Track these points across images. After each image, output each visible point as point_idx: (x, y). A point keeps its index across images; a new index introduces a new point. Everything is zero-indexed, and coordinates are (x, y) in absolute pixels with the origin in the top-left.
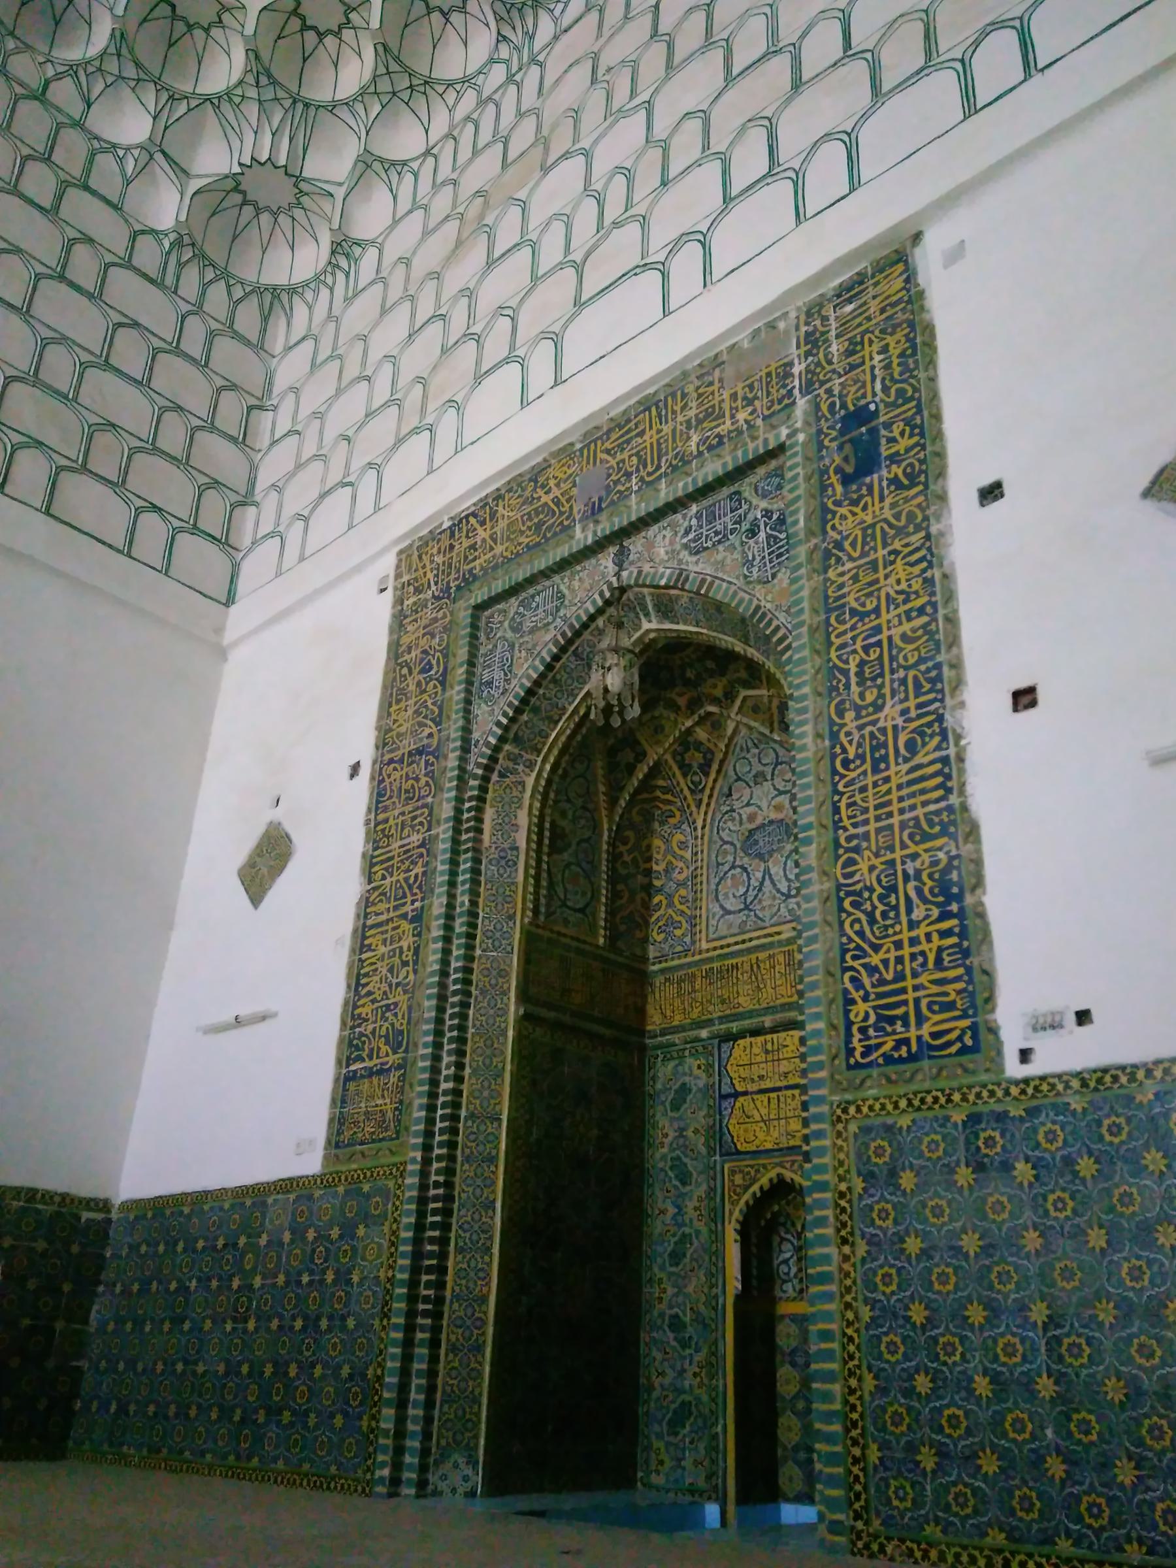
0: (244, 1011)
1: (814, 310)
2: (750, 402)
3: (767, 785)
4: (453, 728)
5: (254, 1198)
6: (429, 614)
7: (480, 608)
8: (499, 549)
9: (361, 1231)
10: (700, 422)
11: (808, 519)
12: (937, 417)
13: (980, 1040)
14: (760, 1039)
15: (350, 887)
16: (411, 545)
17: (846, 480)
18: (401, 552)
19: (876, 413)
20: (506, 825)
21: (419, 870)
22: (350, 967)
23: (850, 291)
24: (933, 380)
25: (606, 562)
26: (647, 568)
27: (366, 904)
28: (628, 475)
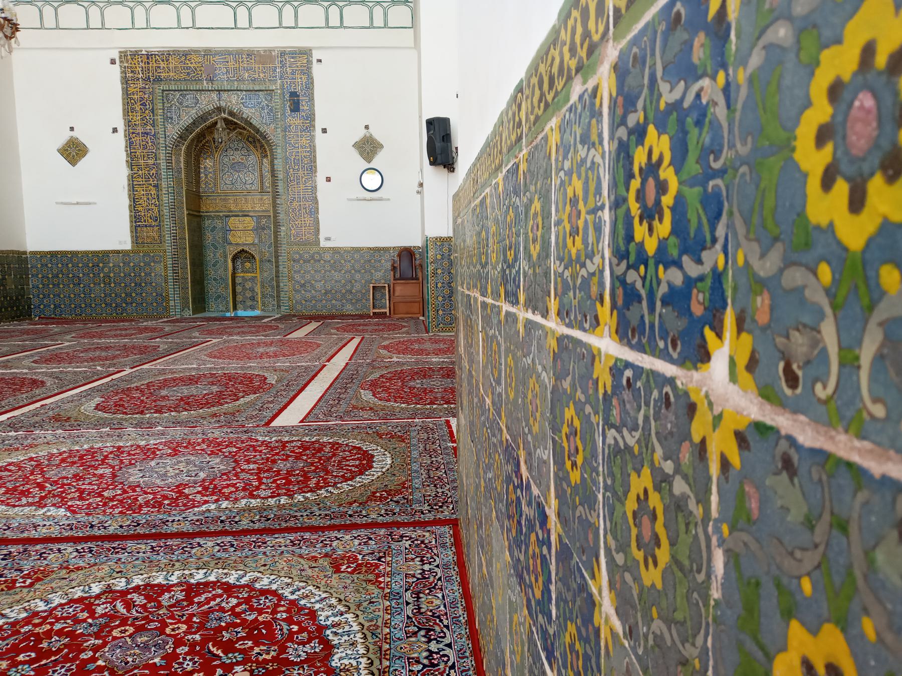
1: (283, 53)
2: (264, 73)
4: (161, 130)
5: (104, 255)
6: (141, 84)
7: (163, 91)
8: (172, 74)
9: (152, 264)
16: (126, 52)
17: (292, 111)
18: (120, 52)
19: (298, 96)
20: (178, 162)
21: (154, 171)
22: (130, 195)
25: (214, 96)
27: (132, 178)
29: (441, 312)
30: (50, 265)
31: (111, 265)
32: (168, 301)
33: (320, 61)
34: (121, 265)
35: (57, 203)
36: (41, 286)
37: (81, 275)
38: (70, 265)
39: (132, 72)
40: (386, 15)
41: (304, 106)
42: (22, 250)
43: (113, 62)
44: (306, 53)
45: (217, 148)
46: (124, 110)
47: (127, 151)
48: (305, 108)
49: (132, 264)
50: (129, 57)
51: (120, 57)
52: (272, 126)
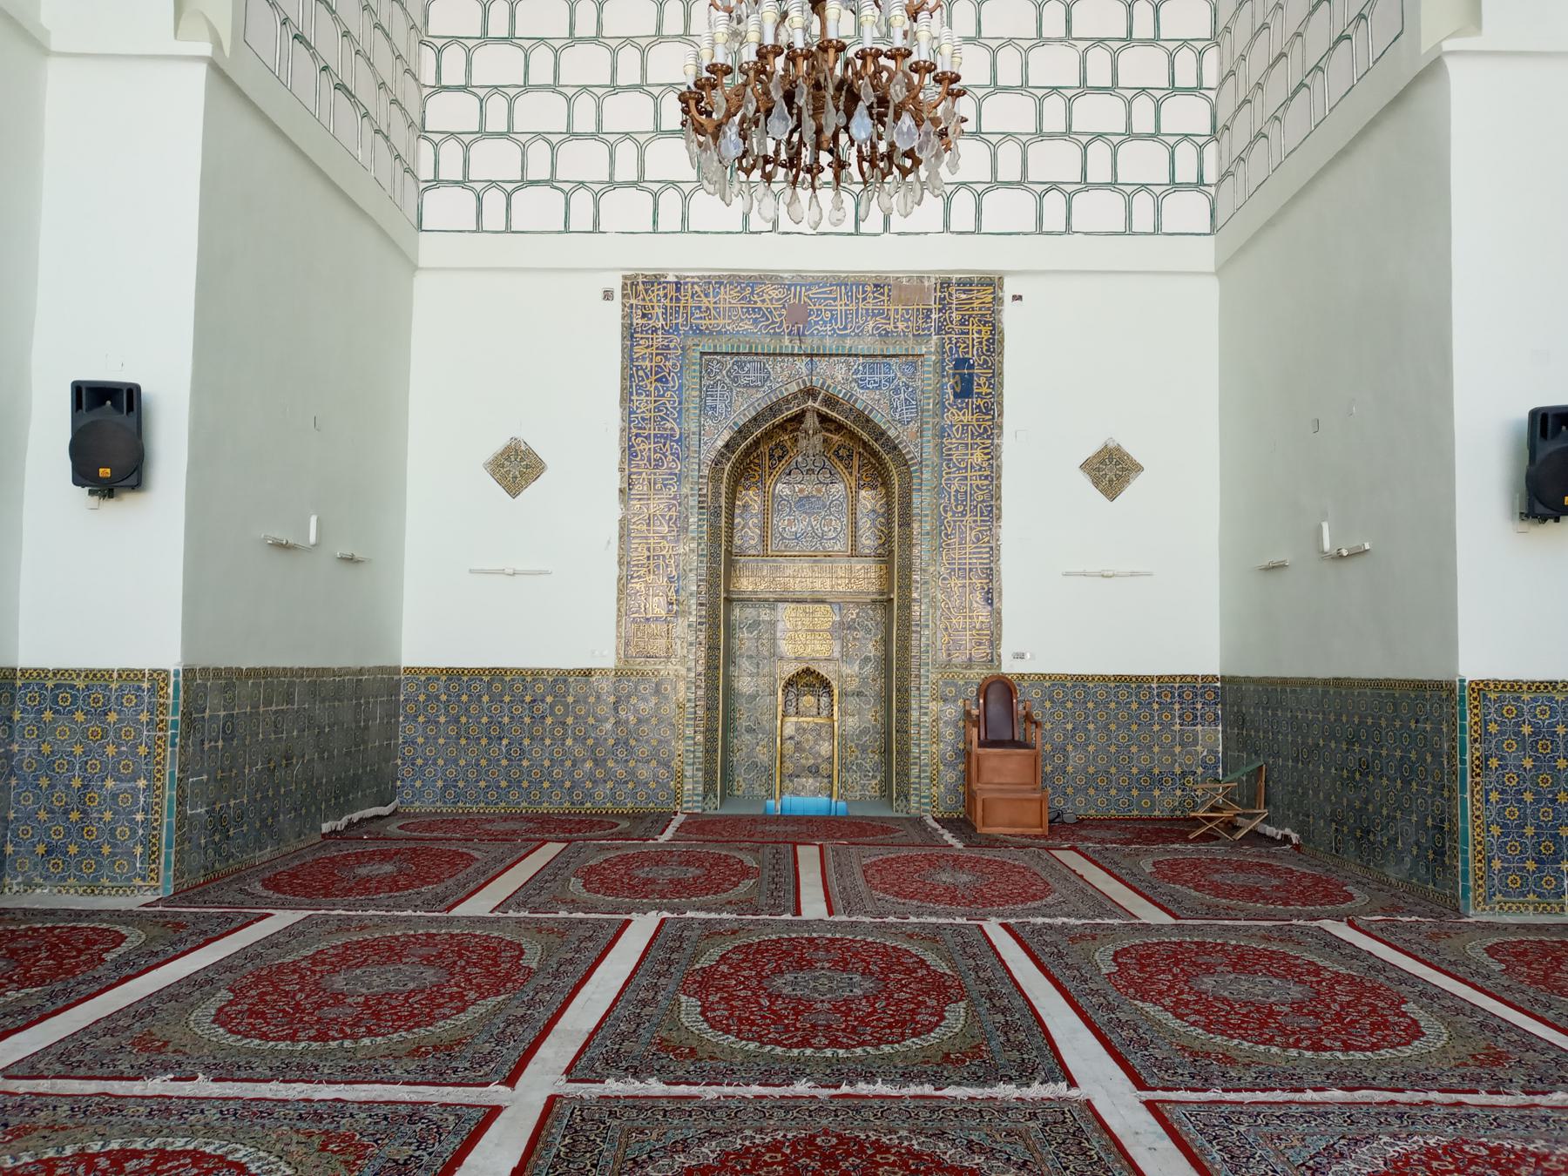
0: (519, 568)
1: (945, 284)
3: (813, 477)
6: (659, 340)
7: (703, 354)
10: (874, 315)
11: (935, 404)
12: (1001, 384)
13: (993, 659)
14: (802, 606)
15: (615, 511)
17: (956, 395)
18: (625, 277)
20: (716, 495)
23: (966, 284)
24: (1001, 363)
25: (802, 365)
26: (829, 382)
28: (825, 323)
29: (1497, 864)
30: (444, 698)
31: (570, 699)
32: (680, 777)
33: (1017, 298)
34: (592, 700)
35: (471, 571)
36: (420, 740)
37: (506, 720)
38: (485, 699)
39: (644, 316)
40: (1158, 211)
41: (981, 385)
42: (393, 664)
43: (608, 295)
44: (992, 283)
45: (772, 467)
46: (623, 389)
47: (622, 470)
48: (984, 390)
49: (612, 699)
50: (641, 287)
51: (624, 287)
52: (914, 426)
